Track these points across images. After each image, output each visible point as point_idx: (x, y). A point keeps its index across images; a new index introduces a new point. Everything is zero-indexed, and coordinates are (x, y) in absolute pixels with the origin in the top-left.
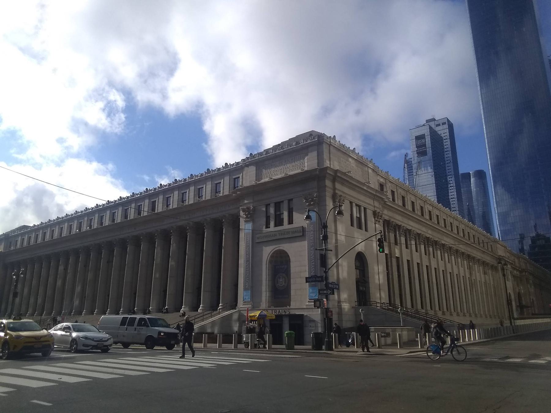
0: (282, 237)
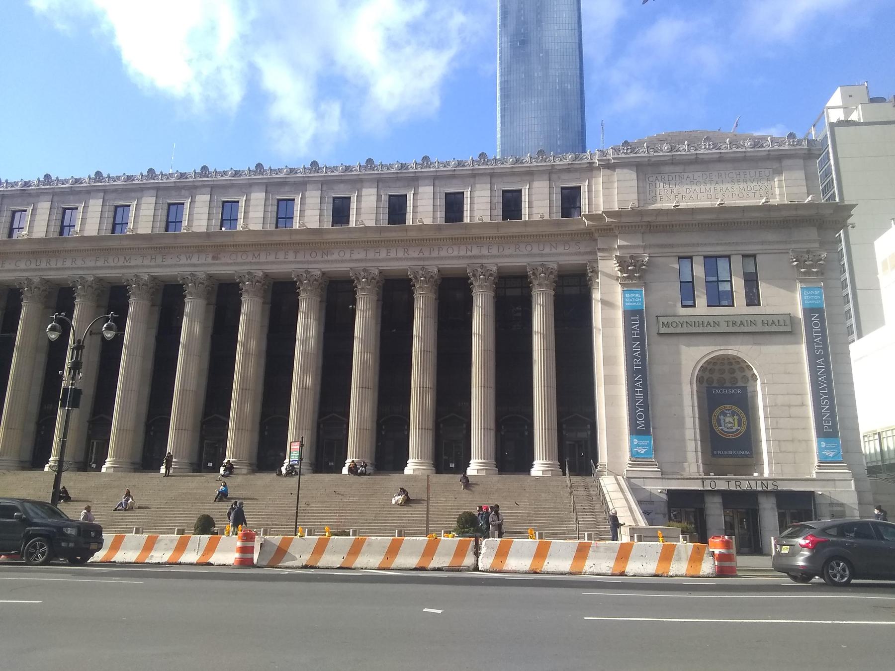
0: (766, 329)
